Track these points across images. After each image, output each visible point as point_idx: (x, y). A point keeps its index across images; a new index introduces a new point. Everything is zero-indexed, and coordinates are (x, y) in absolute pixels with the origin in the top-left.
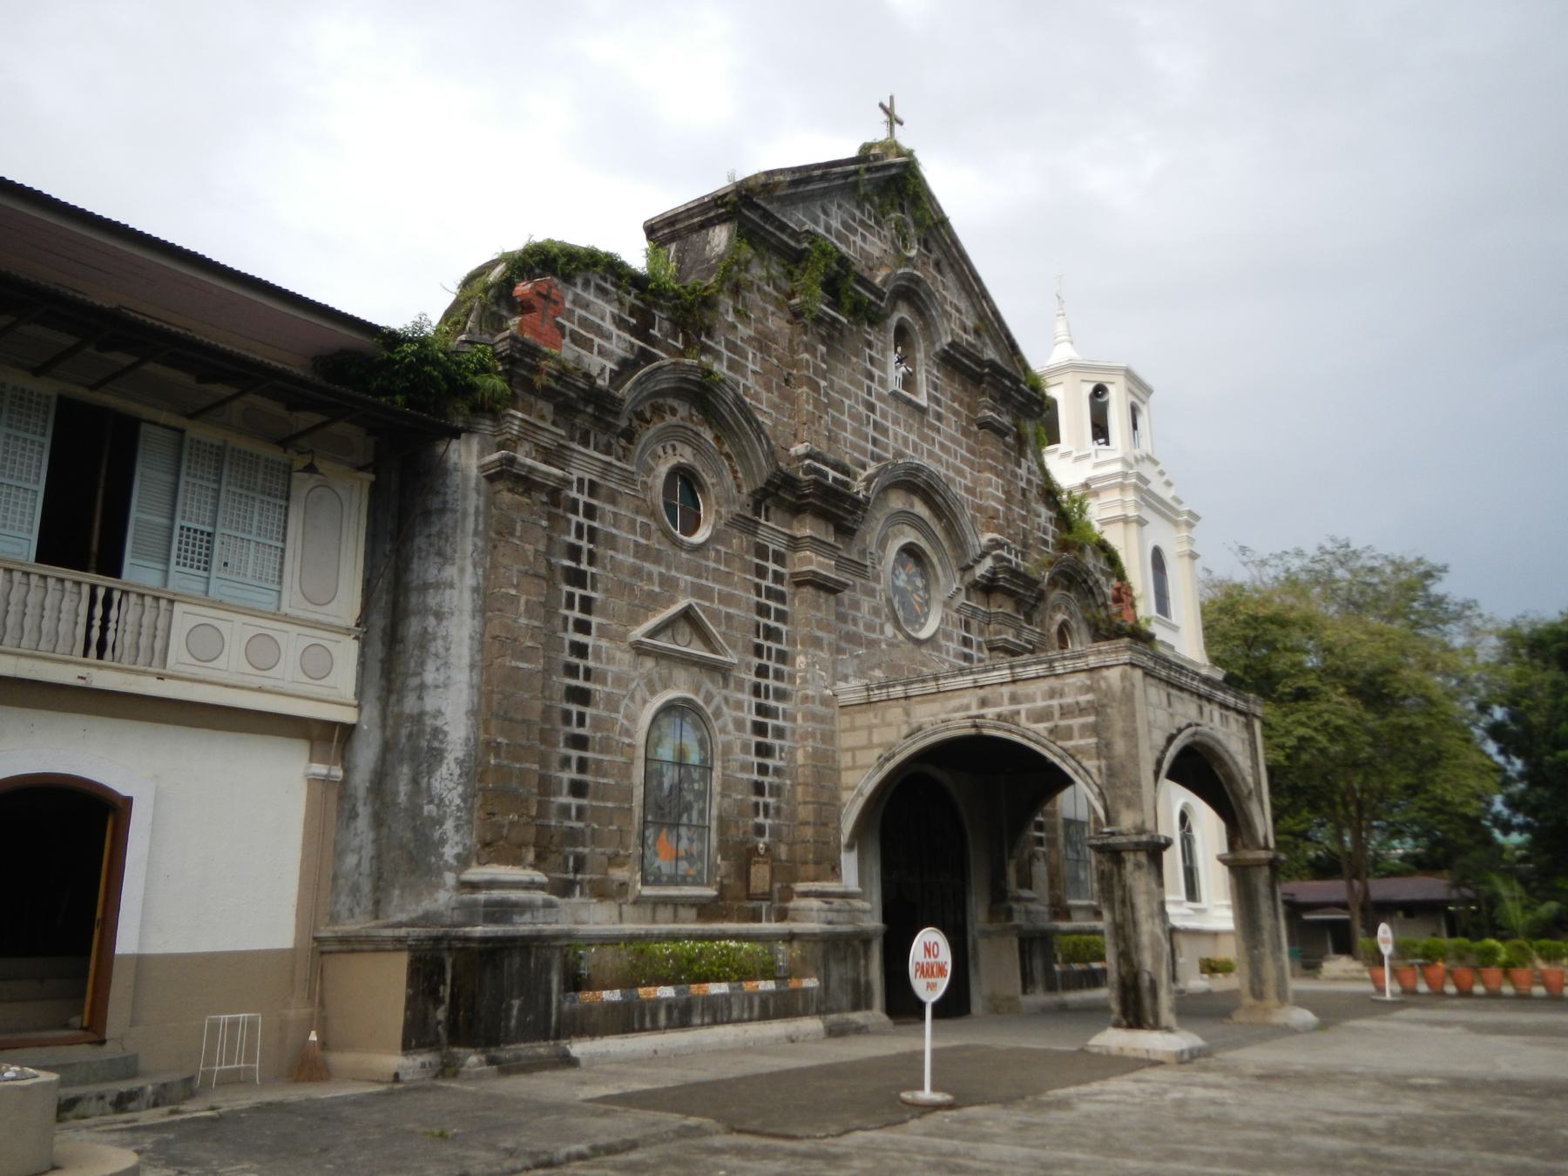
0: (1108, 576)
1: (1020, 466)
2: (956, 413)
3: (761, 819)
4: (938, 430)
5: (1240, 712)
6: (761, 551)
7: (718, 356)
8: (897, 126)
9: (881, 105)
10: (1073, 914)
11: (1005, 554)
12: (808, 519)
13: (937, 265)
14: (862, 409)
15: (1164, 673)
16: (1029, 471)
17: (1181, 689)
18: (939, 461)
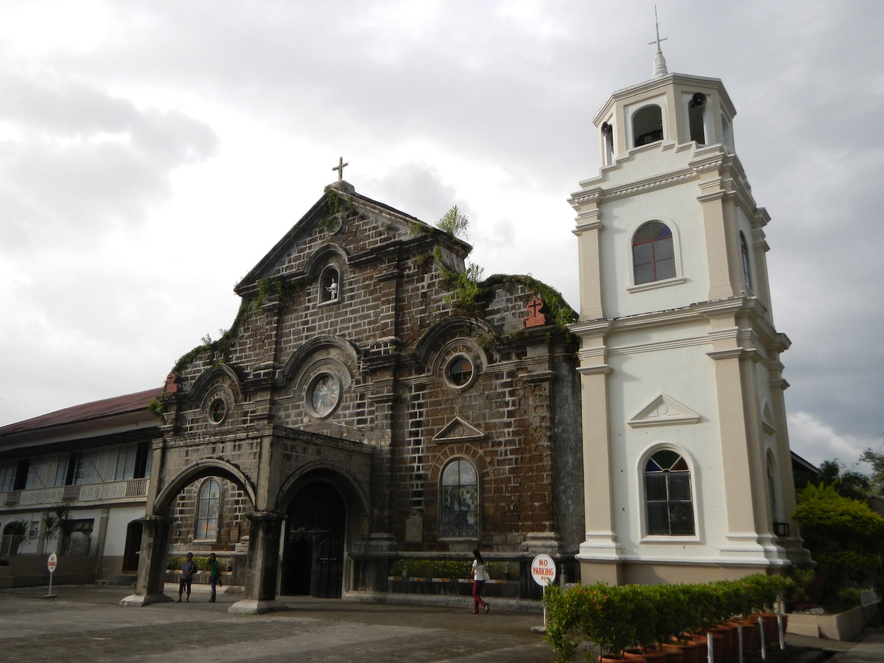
0: (526, 299)
1: (423, 280)
2: (364, 287)
3: (237, 514)
4: (351, 305)
5: (253, 438)
6: (245, 414)
7: (235, 351)
8: (345, 169)
9: (334, 169)
10: (451, 546)
11: (375, 350)
12: (259, 394)
13: (363, 217)
14: (301, 327)
15: (181, 443)
16: (432, 278)
17: (197, 445)
18: (355, 319)
